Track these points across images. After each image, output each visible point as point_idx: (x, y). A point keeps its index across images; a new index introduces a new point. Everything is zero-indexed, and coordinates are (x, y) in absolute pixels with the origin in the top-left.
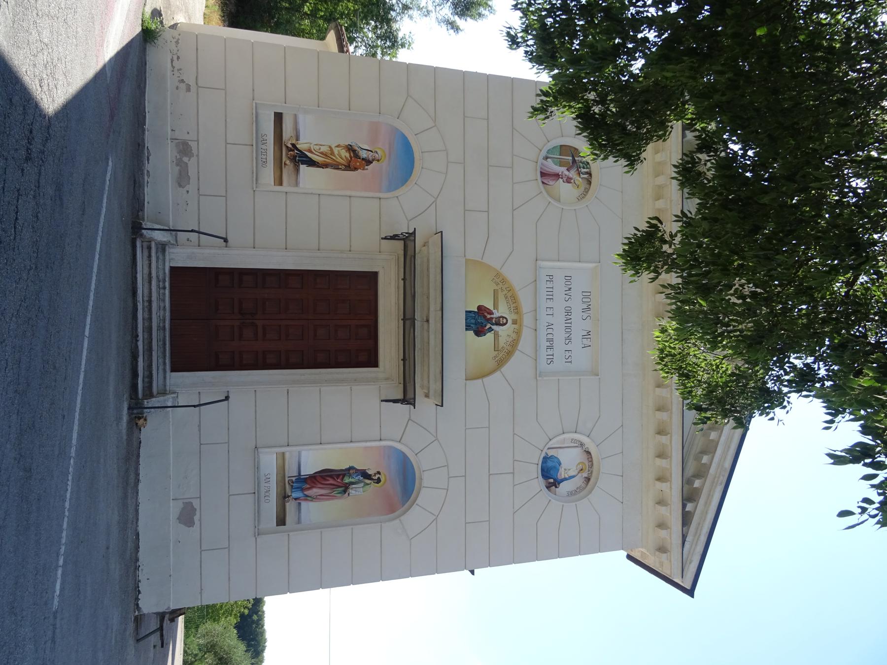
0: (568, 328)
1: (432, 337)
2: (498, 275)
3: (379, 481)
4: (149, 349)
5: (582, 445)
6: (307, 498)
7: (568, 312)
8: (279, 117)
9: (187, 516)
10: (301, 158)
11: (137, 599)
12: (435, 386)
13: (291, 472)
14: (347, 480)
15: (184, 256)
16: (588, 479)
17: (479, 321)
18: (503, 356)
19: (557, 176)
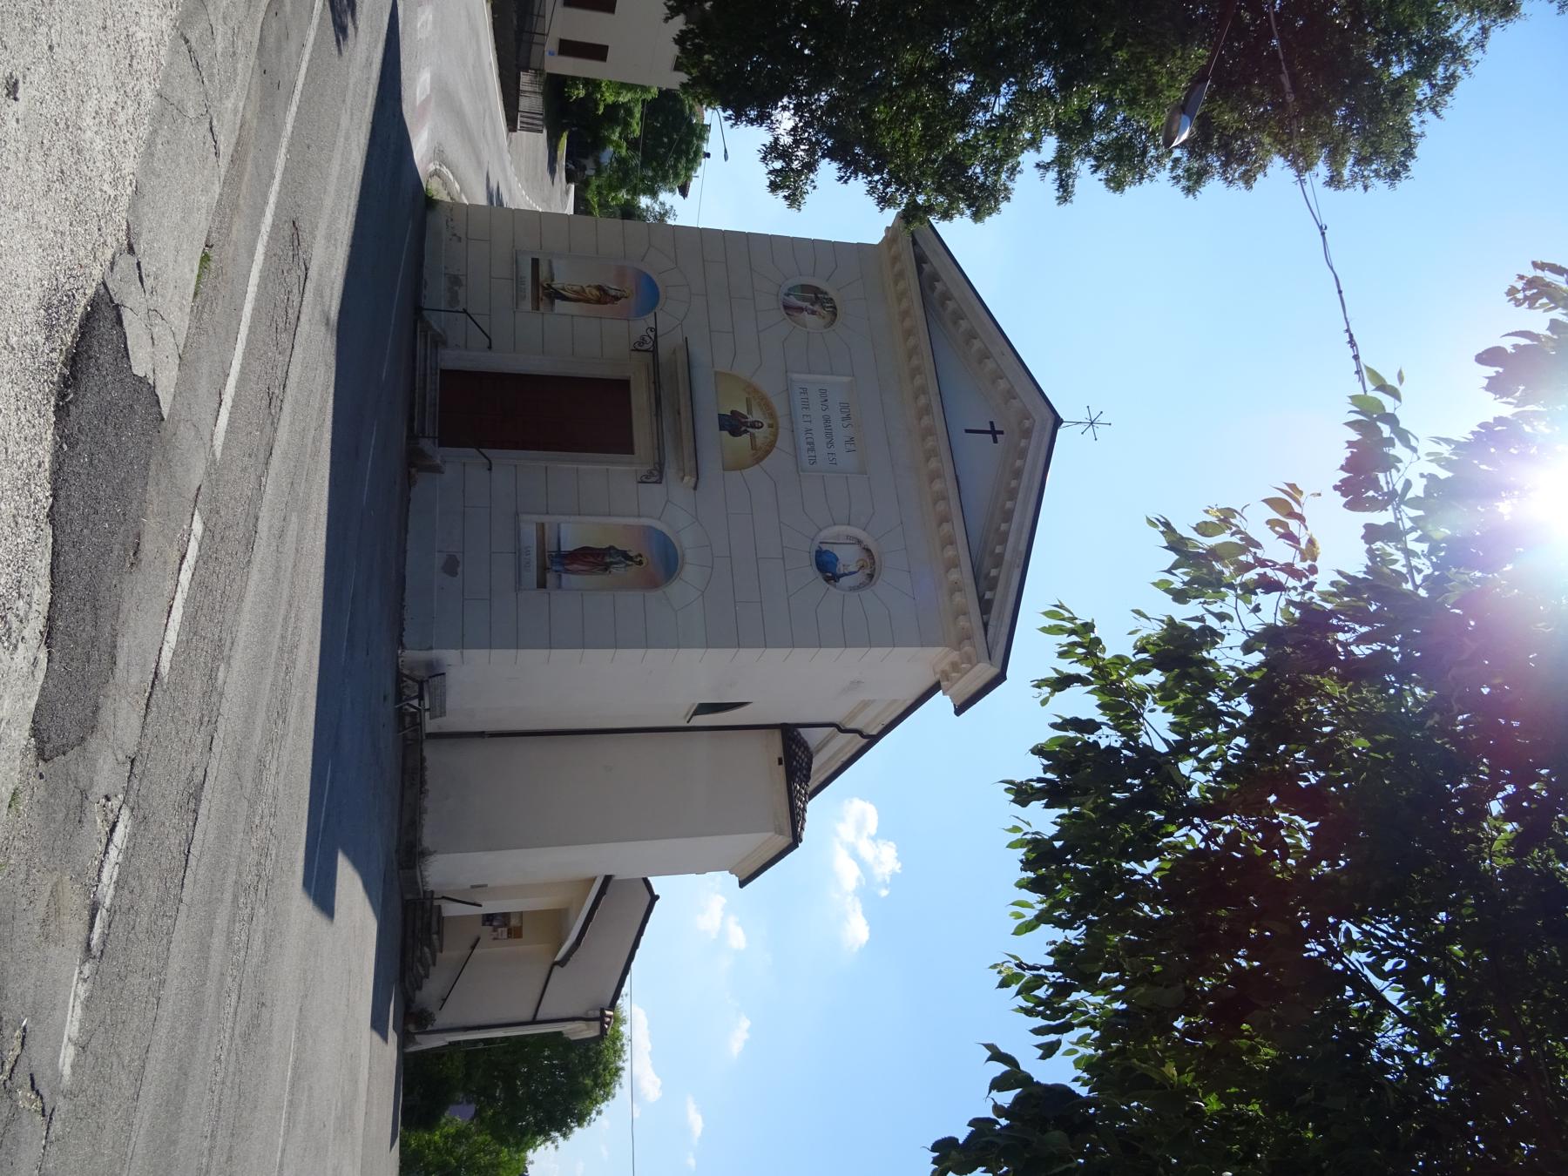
3: (640, 563)
5: (859, 542)
6: (567, 571)
7: (827, 420)
8: (535, 262)
9: (451, 566)
10: (554, 295)
13: (551, 546)
14: (608, 560)
15: (451, 359)
16: (871, 576)
17: (733, 424)
18: (760, 454)
19: (801, 309)
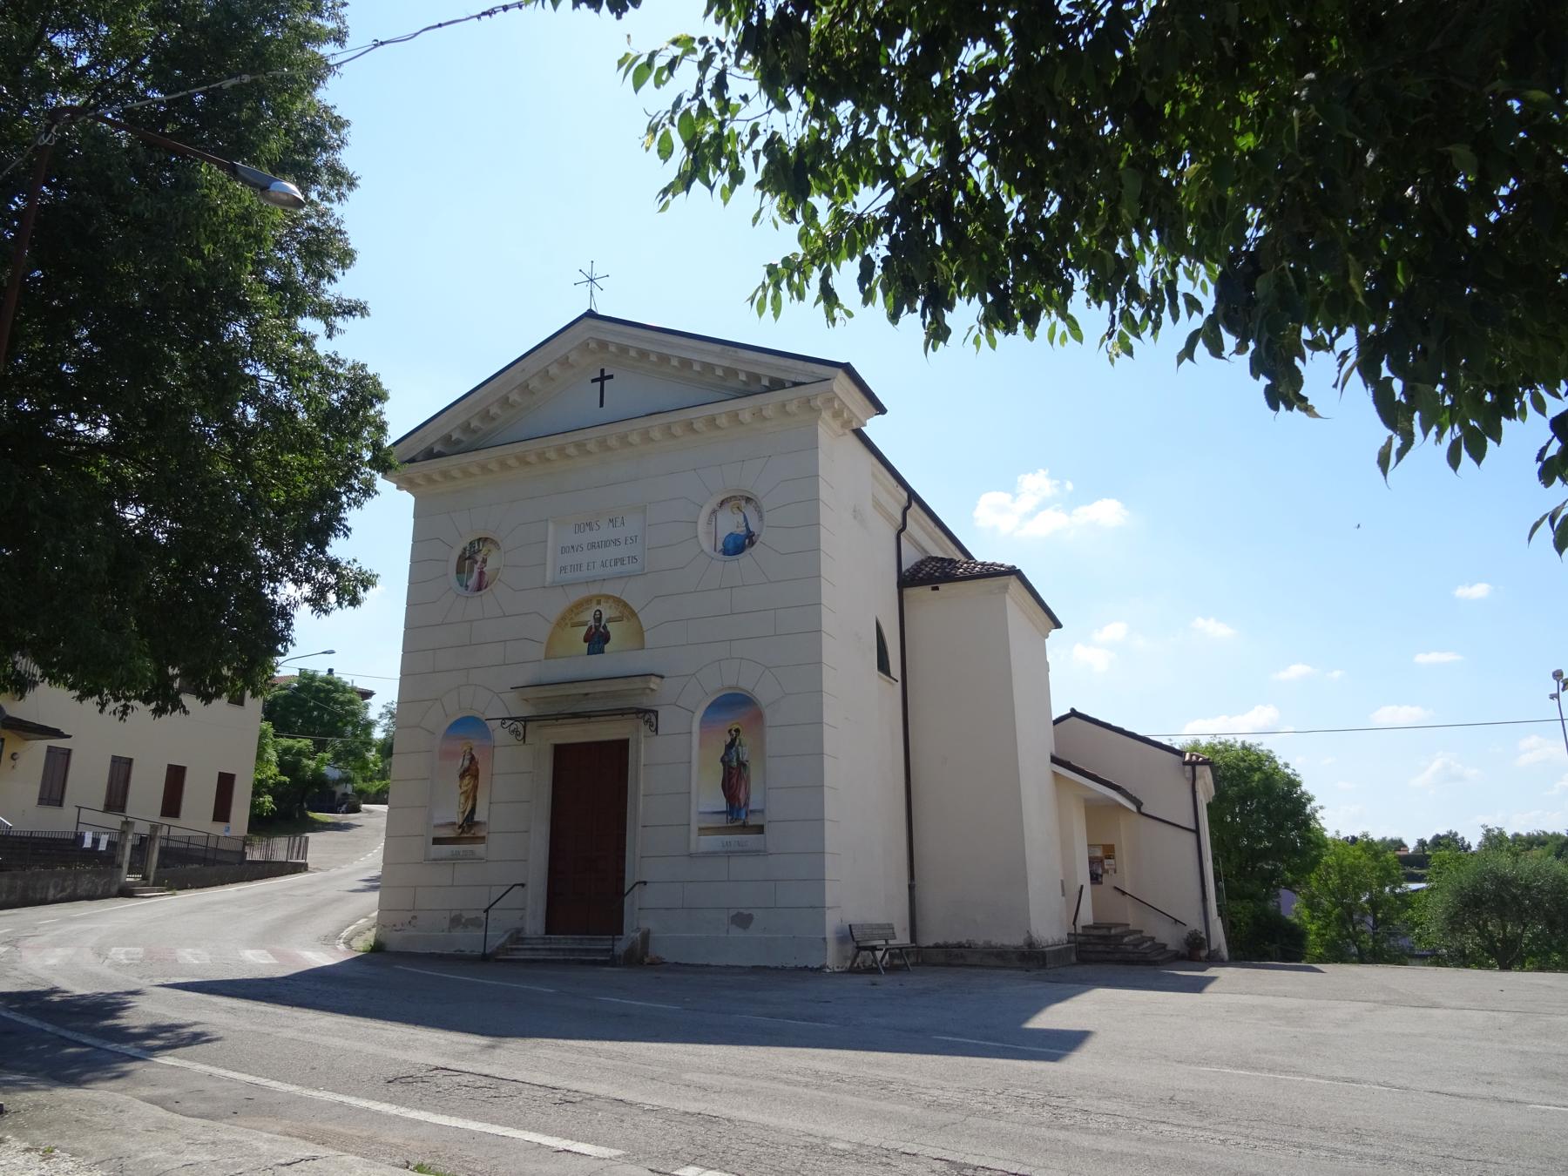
0: (606, 544)
1: (599, 689)
2: (558, 624)
3: (737, 731)
4: (587, 951)
5: (714, 512)
6: (746, 804)
7: (593, 546)
8: (437, 841)
9: (743, 920)
10: (469, 821)
11: (812, 969)
12: (638, 684)
13: (722, 821)
14: (735, 764)
15: (534, 924)
16: (748, 500)
17: (597, 640)
18: (627, 612)
19: (481, 573)
